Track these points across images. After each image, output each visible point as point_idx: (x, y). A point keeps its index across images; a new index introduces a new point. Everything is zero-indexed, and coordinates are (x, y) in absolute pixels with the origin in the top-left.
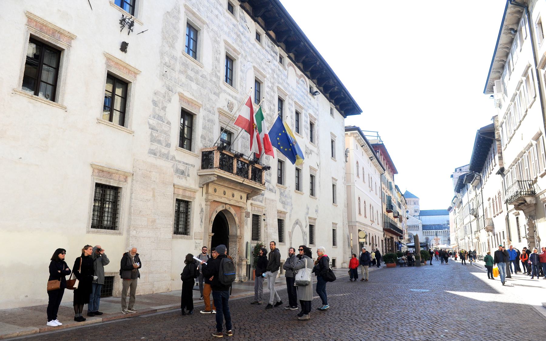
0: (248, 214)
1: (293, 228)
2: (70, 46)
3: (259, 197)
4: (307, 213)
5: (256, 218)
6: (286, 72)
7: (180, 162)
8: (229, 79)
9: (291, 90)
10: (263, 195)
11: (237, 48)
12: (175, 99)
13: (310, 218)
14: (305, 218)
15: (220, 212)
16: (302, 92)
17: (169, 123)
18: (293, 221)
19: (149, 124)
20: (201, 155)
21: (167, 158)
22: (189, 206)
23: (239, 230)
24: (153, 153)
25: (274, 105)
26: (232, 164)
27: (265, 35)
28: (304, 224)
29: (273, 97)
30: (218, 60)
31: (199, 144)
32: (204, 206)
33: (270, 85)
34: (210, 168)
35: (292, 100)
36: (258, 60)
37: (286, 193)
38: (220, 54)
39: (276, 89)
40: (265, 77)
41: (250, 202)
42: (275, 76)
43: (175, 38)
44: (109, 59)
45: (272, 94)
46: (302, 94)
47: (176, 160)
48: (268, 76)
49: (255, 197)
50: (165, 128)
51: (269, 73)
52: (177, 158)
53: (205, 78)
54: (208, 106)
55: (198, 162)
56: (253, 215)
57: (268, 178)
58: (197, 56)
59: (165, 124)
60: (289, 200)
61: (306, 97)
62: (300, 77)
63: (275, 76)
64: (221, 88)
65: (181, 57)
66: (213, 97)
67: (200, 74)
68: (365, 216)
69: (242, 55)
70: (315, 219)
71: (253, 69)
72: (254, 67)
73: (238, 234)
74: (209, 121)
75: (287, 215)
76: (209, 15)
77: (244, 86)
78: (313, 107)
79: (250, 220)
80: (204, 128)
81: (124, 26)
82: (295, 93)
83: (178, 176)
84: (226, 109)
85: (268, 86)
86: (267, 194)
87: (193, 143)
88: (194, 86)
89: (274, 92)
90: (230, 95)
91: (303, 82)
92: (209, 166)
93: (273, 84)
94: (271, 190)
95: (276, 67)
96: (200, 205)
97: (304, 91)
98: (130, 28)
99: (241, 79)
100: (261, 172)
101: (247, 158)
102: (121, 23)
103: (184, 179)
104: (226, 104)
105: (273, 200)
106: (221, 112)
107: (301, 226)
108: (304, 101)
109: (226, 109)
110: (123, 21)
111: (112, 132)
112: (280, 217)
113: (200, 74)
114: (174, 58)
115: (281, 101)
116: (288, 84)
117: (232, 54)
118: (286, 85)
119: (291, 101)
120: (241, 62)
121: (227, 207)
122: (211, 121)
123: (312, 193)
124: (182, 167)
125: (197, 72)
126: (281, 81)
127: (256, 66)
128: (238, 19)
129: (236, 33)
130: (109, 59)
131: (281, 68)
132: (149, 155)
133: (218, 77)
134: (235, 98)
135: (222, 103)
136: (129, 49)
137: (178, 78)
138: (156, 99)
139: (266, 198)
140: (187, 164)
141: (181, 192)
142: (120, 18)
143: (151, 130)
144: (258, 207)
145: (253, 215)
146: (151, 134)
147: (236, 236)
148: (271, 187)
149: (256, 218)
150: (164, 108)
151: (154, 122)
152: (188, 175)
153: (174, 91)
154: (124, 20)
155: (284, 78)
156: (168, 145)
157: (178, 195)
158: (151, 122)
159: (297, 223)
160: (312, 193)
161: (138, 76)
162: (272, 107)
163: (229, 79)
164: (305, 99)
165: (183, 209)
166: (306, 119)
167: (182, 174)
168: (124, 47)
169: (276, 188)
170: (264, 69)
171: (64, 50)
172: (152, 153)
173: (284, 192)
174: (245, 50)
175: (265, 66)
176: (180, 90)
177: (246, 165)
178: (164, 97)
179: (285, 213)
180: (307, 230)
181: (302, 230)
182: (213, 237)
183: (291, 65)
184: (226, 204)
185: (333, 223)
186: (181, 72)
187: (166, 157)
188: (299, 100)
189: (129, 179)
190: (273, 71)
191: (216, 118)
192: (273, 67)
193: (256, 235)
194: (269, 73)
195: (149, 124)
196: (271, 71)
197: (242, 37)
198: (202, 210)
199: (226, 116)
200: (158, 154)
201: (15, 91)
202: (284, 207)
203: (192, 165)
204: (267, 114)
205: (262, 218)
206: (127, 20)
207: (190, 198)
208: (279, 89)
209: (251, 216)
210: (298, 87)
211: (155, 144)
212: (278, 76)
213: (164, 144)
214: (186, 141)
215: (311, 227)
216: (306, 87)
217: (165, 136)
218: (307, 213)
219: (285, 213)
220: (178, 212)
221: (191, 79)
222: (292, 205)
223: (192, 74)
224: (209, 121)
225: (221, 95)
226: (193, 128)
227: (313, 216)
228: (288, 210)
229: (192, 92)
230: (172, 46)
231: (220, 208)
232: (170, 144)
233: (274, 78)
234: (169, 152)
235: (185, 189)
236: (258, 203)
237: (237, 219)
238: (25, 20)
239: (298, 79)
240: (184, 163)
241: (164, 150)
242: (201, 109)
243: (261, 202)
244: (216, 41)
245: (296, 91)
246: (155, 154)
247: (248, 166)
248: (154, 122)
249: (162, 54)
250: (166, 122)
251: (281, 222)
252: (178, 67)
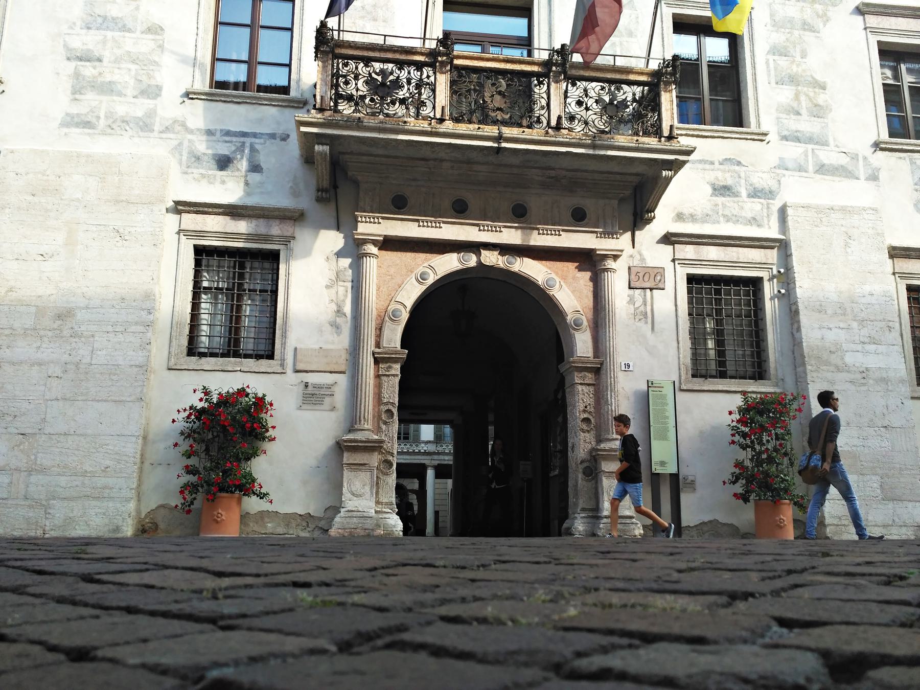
0: (646, 280)
17: (154, 30)
59: (138, 34)
132: (65, 130)
140: (244, 134)
148: (829, 156)
156: (151, 92)
157: (200, 234)
172: (77, 125)
200: (102, 123)
203: (273, 136)
217: (133, 67)
231: (449, 263)
232: (159, 88)
234: (151, 114)
240: (228, 133)
243: (753, 221)
246: (87, 124)
248: (84, 41)
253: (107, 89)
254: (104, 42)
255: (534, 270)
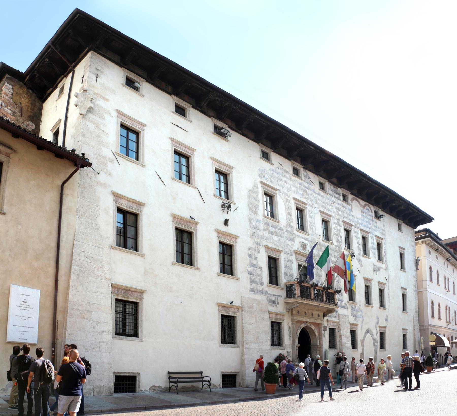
0: (325, 329)
1: (365, 336)
2: (196, 229)
3: (334, 314)
4: (377, 323)
5: (332, 332)
6: (350, 207)
7: (271, 295)
8: (302, 226)
9: (356, 220)
10: (337, 312)
11: (305, 201)
12: (263, 250)
13: (380, 327)
14: (376, 327)
15: (304, 328)
16: (368, 218)
17: (260, 268)
18: (365, 331)
19: (248, 271)
20: (285, 288)
21: (262, 293)
22: (281, 326)
23: (318, 341)
24: (252, 290)
25: (341, 237)
26: (310, 292)
27: (327, 183)
28: (374, 332)
29: (340, 231)
30: (290, 214)
31: (283, 280)
32: (290, 325)
33: (336, 221)
34: (294, 297)
35: (358, 228)
36: (324, 205)
37: (357, 308)
38: (291, 209)
39: (341, 223)
40: (330, 216)
41: (326, 318)
42: (340, 213)
43: (257, 207)
44: (219, 232)
45: (339, 228)
46: (367, 220)
47: (268, 294)
48: (333, 215)
49: (330, 315)
50: (258, 272)
51: (334, 212)
52: (269, 292)
53: (282, 230)
54: (287, 250)
55: (283, 293)
56: (329, 329)
57: (340, 298)
58: (274, 214)
60: (360, 314)
61: (371, 222)
62: (364, 207)
63: (340, 213)
64: (295, 235)
65: (263, 219)
66: (290, 243)
67: (278, 228)
68: (440, 318)
69: (309, 204)
70: (385, 327)
71: (319, 213)
72: (320, 211)
73: (318, 344)
74: (288, 261)
75: (359, 326)
76: (279, 183)
77: (314, 228)
78: (379, 228)
79: (327, 333)
80: (286, 267)
81: (224, 209)
82: (360, 222)
83: (271, 305)
84: (301, 250)
85: (334, 223)
86: (340, 311)
87: (278, 279)
88: (275, 238)
89: (340, 226)
90: (302, 238)
91: (368, 210)
92: (293, 295)
93: (339, 219)
94: (343, 307)
95: (340, 205)
96: (288, 324)
97: (369, 217)
98: (228, 209)
99: (311, 223)
100: (334, 295)
101: (320, 286)
102: (222, 207)
103: (275, 307)
104: (300, 246)
105: (345, 316)
106: (297, 253)
107: (372, 334)
108: (369, 226)
109: (301, 250)
110: (223, 205)
111: (225, 280)
112: (353, 328)
113: (278, 228)
114: (258, 221)
115: (347, 232)
116: (353, 216)
117: (301, 206)
118: (351, 217)
119: (356, 230)
120: (309, 211)
121: (308, 324)
122: (290, 261)
123: (382, 304)
124: (273, 298)
125: (276, 227)
126: (345, 215)
127: (322, 210)
128: (303, 178)
129: (303, 190)
130: (219, 232)
131: (345, 205)
133: (292, 227)
134: (307, 240)
135: (296, 246)
136: (230, 223)
137: (263, 235)
138: (249, 253)
139: (339, 314)
140: (276, 295)
141: (274, 316)
142: (221, 203)
143: (249, 275)
144: (333, 322)
145: (329, 329)
146: (250, 278)
147: (317, 345)
149: (332, 332)
150: (256, 258)
151: (250, 269)
152: (278, 304)
153: (261, 244)
154: (224, 205)
155: (348, 212)
156: (262, 284)
158: (249, 269)
159: (368, 331)
160: (382, 304)
161: (238, 240)
162: (340, 239)
163: (302, 226)
164: (370, 224)
165: (276, 327)
166: (373, 241)
167: (273, 303)
168: (226, 222)
169: (348, 305)
170: (329, 210)
171: (193, 232)
173: (355, 307)
174: (311, 200)
175: (330, 208)
176: (265, 243)
177: (321, 291)
178: (255, 250)
179: (357, 325)
180: (378, 337)
181: (373, 337)
182: (299, 347)
183: (353, 199)
184: (307, 322)
185: (403, 329)
186: (264, 230)
187: (261, 292)
188: (365, 226)
189: (240, 310)
190: (338, 209)
191: (293, 258)
192: (337, 206)
193: (332, 345)
194: (334, 212)
195: (248, 271)
196: (335, 210)
197: (308, 191)
198: (290, 327)
199: (301, 255)
200: (256, 291)
201: (173, 263)
202: (356, 320)
203: (280, 296)
204: (336, 246)
205: (337, 331)
206: (226, 204)
207: (280, 319)
208: (344, 222)
209: (328, 330)
210: (363, 216)
211: (253, 284)
212: (343, 212)
213: (259, 284)
214: (274, 278)
215: (382, 335)
216: (370, 213)
218: (377, 323)
219: (357, 325)
220: (272, 330)
221: (272, 233)
222: (363, 317)
223: (271, 229)
224: (288, 261)
225: (295, 240)
226: (278, 268)
227: (382, 323)
228: (359, 322)
229: (274, 242)
230: (256, 213)
231: (303, 326)
233: (339, 215)
234: (263, 289)
235: (276, 314)
236: (333, 319)
237: (316, 333)
238: (171, 219)
239: (362, 209)
240: (274, 295)
241: (260, 288)
242: (282, 254)
243: (335, 317)
244: (288, 201)
245: (362, 220)
246: (254, 291)
247: (322, 292)
248: (250, 269)
249: (250, 220)
250: (258, 267)
251: (353, 333)
252: (262, 226)
253: (256, 282)
254: (253, 270)
255: (313, 327)
